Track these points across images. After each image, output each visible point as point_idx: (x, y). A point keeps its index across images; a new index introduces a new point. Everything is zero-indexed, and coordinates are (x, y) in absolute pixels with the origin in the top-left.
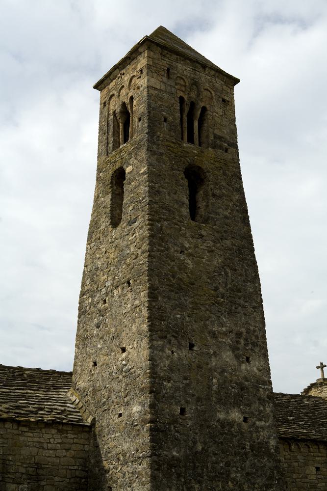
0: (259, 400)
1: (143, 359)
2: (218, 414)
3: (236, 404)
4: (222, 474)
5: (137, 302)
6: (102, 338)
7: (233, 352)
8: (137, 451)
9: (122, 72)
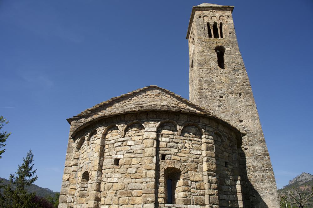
1: (257, 128)
5: (248, 103)
6: (224, 112)
8: (263, 166)
9: (214, 11)
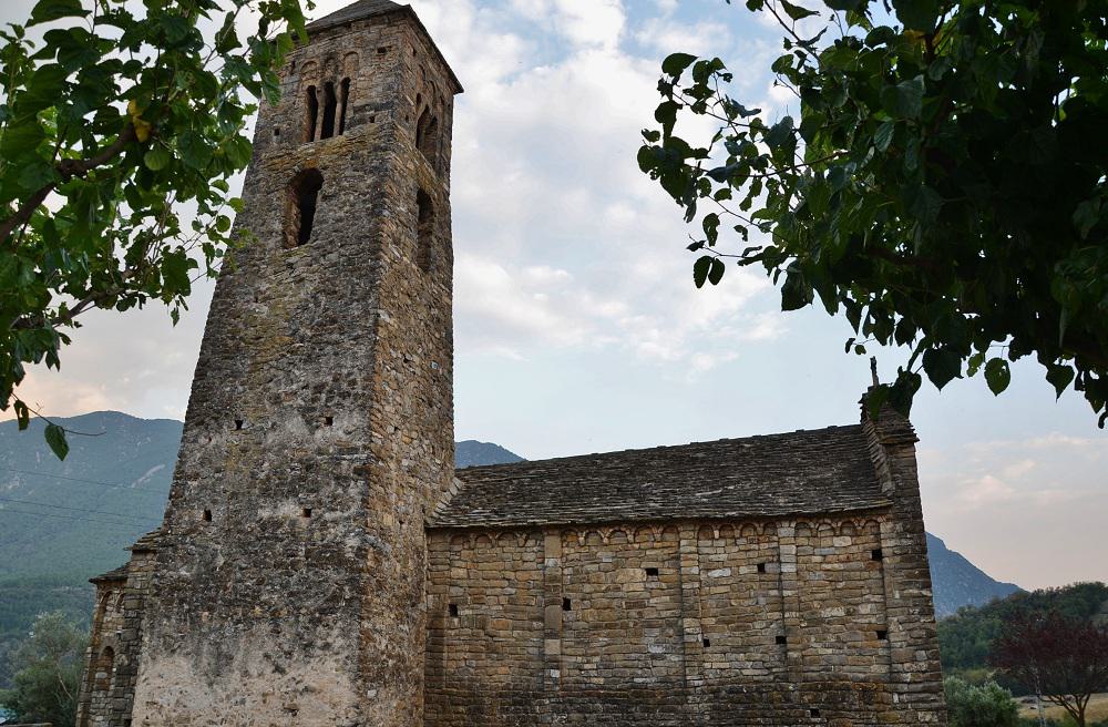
0: (337, 478)
2: (260, 511)
3: (293, 493)
4: (247, 595)
7: (303, 416)
